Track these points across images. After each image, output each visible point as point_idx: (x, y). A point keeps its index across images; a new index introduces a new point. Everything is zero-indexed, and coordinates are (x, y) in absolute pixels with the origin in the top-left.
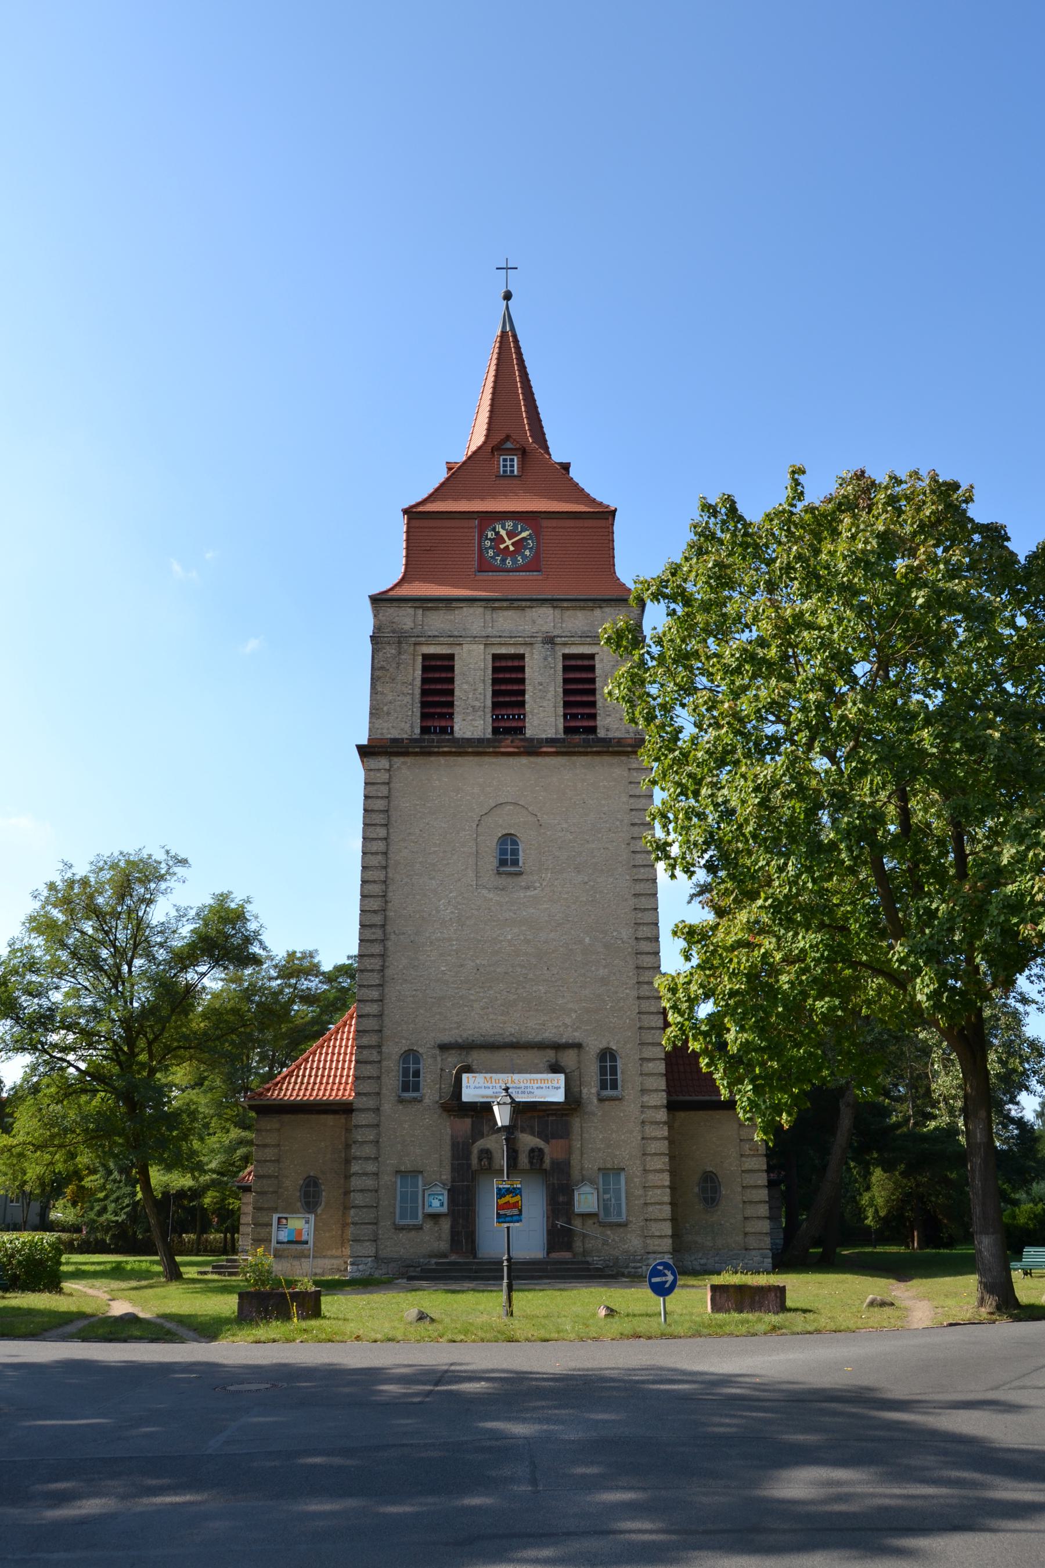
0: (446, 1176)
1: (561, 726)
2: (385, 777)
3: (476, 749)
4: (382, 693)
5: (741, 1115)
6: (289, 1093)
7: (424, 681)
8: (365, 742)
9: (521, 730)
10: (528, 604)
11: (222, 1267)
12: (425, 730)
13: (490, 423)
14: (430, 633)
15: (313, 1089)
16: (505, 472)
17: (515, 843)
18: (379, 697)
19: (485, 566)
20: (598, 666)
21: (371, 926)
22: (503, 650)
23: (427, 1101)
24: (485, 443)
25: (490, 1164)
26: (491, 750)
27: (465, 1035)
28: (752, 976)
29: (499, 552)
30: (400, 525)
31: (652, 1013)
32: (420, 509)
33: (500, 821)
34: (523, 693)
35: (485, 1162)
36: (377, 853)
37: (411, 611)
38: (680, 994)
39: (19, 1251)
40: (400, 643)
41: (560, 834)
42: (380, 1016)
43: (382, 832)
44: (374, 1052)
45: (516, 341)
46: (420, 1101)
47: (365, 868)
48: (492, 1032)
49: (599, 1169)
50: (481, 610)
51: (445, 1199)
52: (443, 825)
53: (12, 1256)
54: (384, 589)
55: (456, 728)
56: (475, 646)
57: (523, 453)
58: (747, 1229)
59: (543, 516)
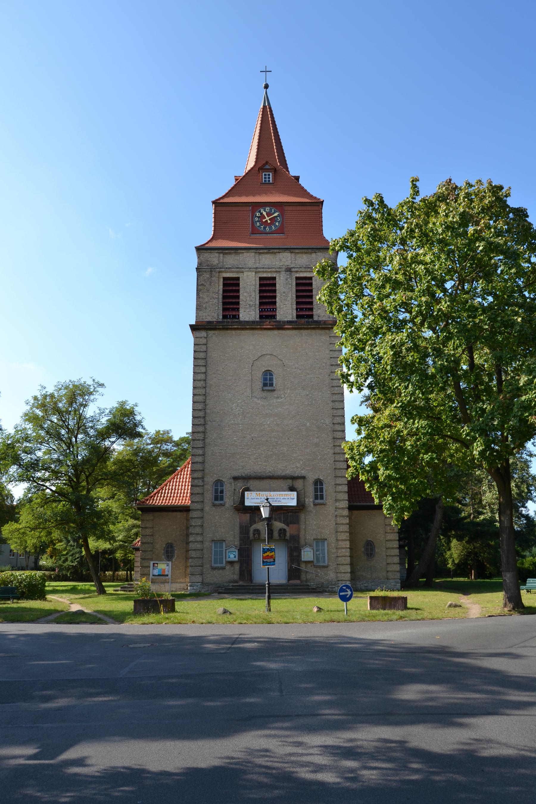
0: (237, 543)
1: (295, 315)
2: (204, 341)
3: (251, 327)
4: (203, 298)
5: (385, 512)
6: (157, 501)
7: (224, 291)
8: (194, 323)
9: (274, 317)
10: (278, 251)
11: (125, 587)
12: (224, 317)
13: (257, 155)
14: (227, 266)
15: (169, 500)
16: (265, 181)
17: (271, 375)
19: (255, 231)
21: (198, 417)
22: (265, 275)
23: (227, 505)
24: (255, 166)
25: (259, 536)
26: (259, 327)
27: (246, 473)
28: (391, 442)
29: (262, 223)
30: (211, 209)
32: (221, 201)
33: (264, 364)
34: (275, 297)
35: (256, 536)
36: (200, 380)
37: (217, 255)
38: (355, 451)
39: (24, 580)
40: (211, 271)
42: (203, 463)
43: (203, 369)
44: (200, 481)
45: (271, 111)
46: (224, 505)
47: (194, 388)
48: (260, 471)
49: (314, 539)
50: (253, 254)
51: (237, 554)
53: (21, 582)
54: (203, 243)
55: (241, 316)
56: (250, 273)
57: (275, 171)
58: (388, 569)
59: (285, 204)
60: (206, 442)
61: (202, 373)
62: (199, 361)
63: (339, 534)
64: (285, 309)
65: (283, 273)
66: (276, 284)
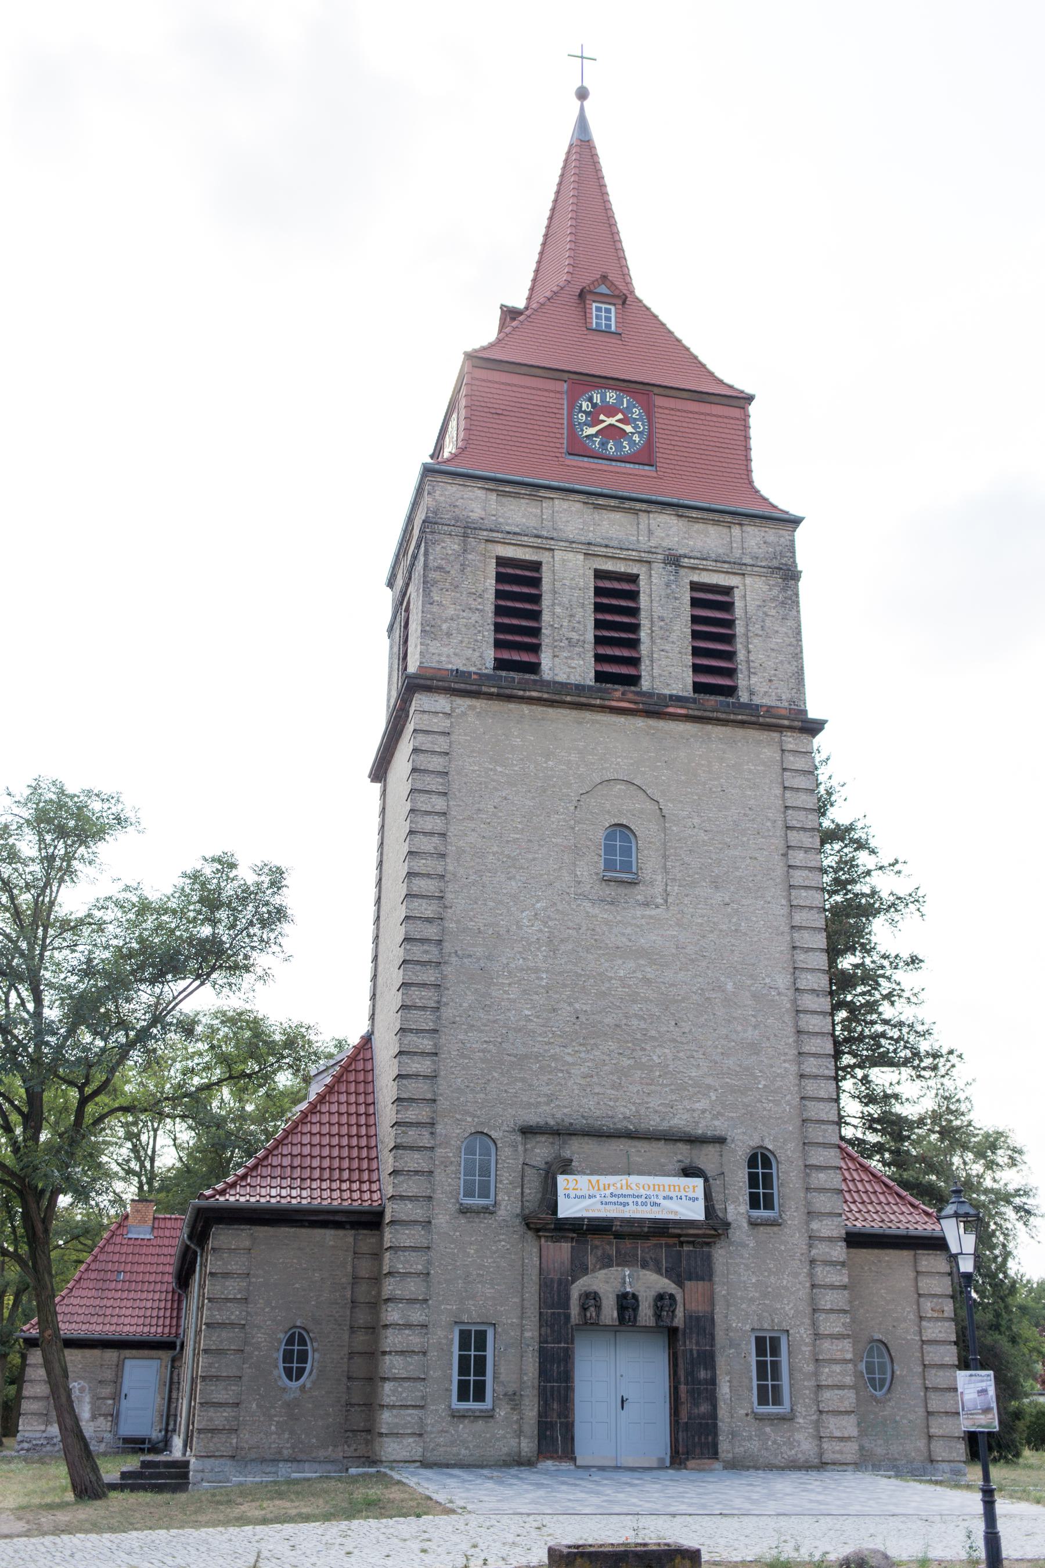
2: (443, 724)
4: (440, 604)
9: (634, 680)
10: (644, 506)
14: (508, 528)
18: (435, 609)
20: (738, 604)
22: (609, 566)
23: (502, 1212)
25: (598, 1315)
26: (598, 702)
27: (559, 1115)
31: (822, 1100)
33: (608, 806)
36: (432, 834)
37: (481, 493)
40: (465, 536)
41: (690, 831)
42: (432, 1077)
48: (598, 1113)
50: (579, 505)
52: (528, 802)
56: (571, 555)
59: (656, 390)
60: (444, 1016)
61: (437, 813)
62: (428, 778)
63: (822, 1317)
64: (664, 662)
65: (658, 568)
66: (638, 592)
